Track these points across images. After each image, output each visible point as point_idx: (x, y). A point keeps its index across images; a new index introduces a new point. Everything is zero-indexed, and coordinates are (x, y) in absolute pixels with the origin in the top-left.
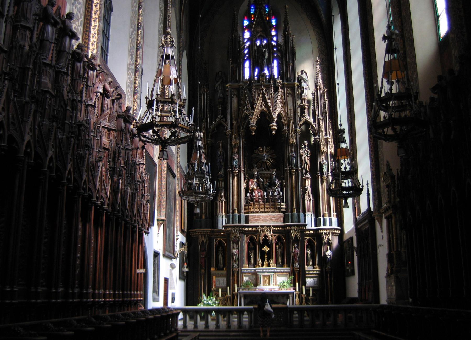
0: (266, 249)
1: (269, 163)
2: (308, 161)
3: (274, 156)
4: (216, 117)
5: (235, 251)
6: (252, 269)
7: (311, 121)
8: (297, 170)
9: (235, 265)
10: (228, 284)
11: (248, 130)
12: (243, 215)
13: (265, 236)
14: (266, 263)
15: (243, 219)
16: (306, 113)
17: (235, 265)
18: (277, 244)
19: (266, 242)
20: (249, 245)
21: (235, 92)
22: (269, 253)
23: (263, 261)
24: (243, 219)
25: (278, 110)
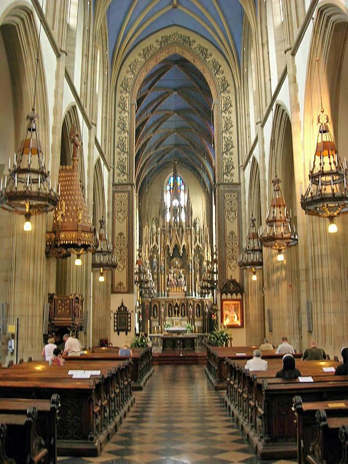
0: (177, 309)
1: (179, 266)
2: (198, 265)
3: (182, 262)
4: (153, 242)
5: (163, 310)
6: (170, 318)
7: (201, 245)
8: (192, 271)
9: (163, 316)
10: (159, 325)
11: (169, 254)
12: (166, 293)
13: (177, 303)
14: (177, 315)
15: (166, 295)
16: (198, 241)
17: (163, 316)
18: (182, 306)
19: (177, 305)
20: (169, 307)
21: (162, 232)
22: (178, 311)
23: (175, 314)
24: (166, 295)
25: (184, 243)
